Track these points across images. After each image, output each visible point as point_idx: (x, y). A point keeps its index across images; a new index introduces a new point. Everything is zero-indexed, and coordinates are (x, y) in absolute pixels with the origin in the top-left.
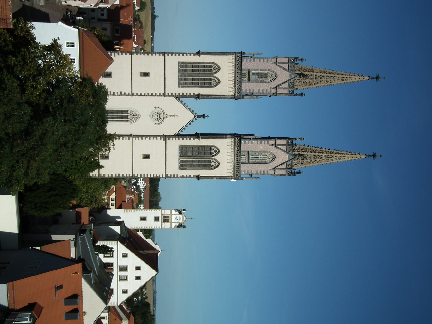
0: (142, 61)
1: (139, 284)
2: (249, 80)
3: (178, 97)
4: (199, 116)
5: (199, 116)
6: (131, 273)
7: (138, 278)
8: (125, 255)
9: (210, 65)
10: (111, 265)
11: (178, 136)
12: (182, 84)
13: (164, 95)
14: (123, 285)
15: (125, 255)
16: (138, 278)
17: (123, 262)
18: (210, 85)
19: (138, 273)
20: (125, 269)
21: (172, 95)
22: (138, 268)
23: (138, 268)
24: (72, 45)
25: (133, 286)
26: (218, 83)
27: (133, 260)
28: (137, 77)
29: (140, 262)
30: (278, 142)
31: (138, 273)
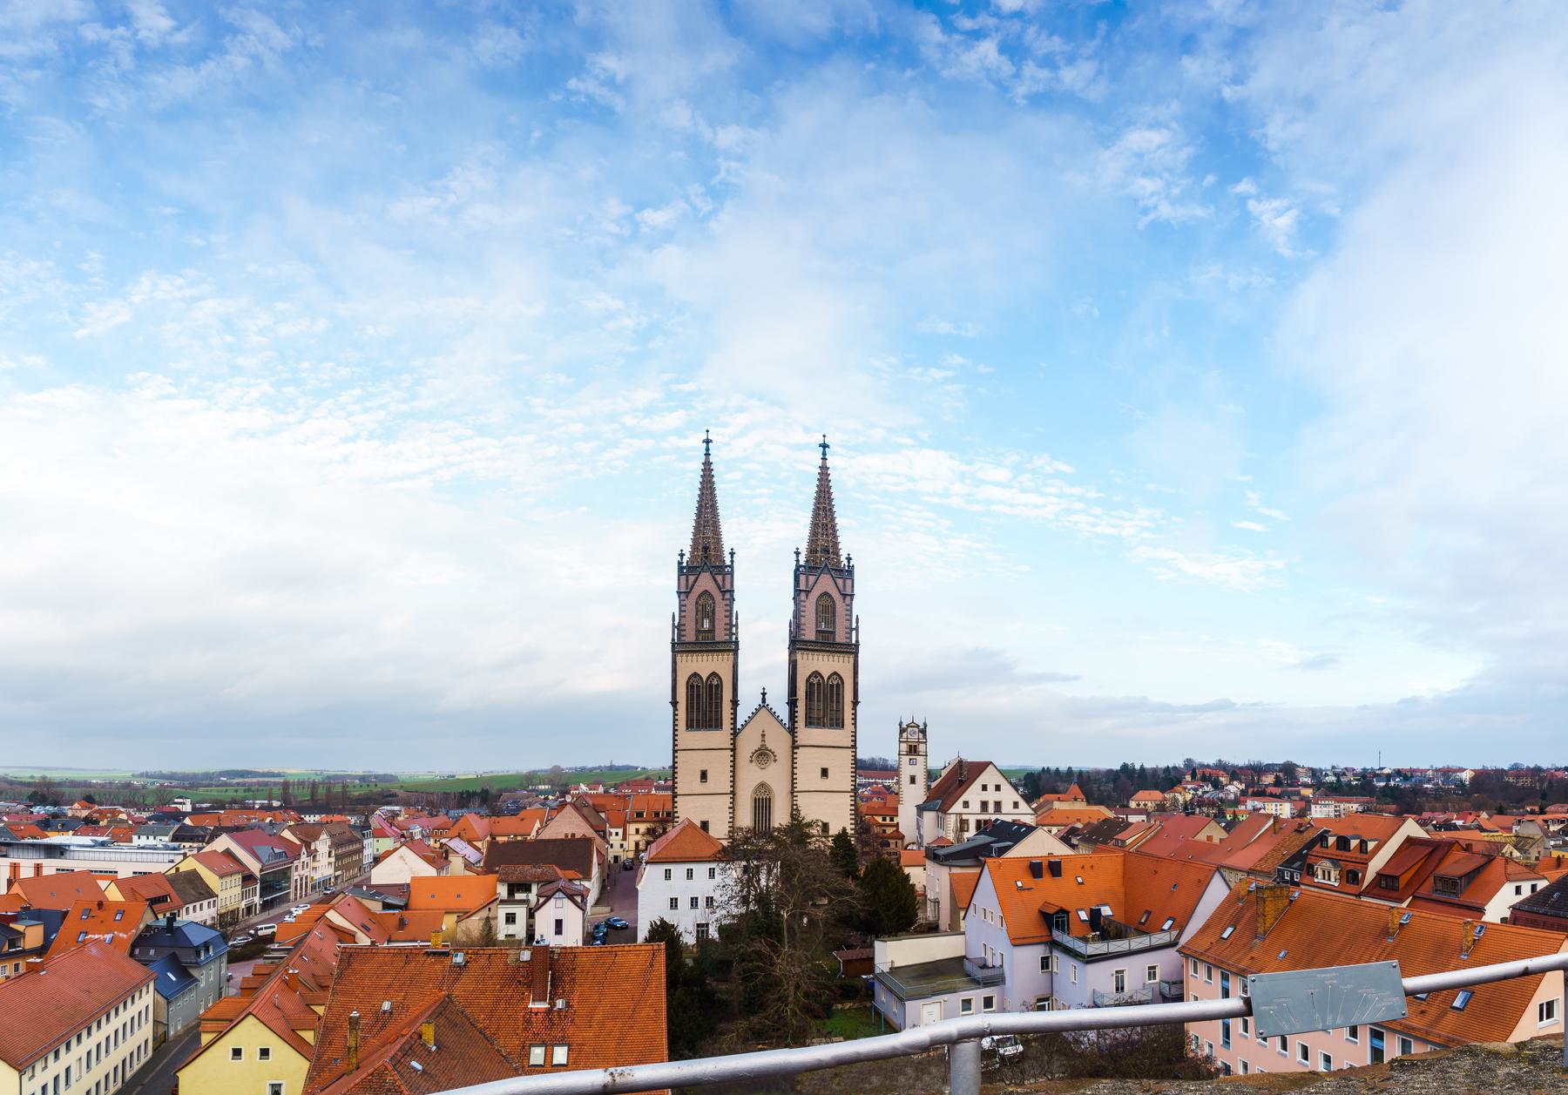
0: (687, 781)
1: (1006, 787)
2: (712, 630)
3: (735, 733)
4: (764, 700)
5: (764, 700)
6: (991, 796)
7: (998, 788)
8: (966, 804)
9: (690, 686)
10: (978, 822)
11: (792, 730)
12: (718, 725)
13: (733, 750)
14: (1007, 807)
15: (966, 804)
16: (998, 788)
17: (975, 806)
18: (720, 686)
19: (991, 788)
20: (984, 805)
21: (734, 739)
22: (984, 788)
23: (984, 788)
24: (668, 872)
25: (1009, 796)
26: (714, 674)
27: (973, 795)
28: (709, 786)
29: (976, 786)
30: (802, 587)
31: (991, 788)
